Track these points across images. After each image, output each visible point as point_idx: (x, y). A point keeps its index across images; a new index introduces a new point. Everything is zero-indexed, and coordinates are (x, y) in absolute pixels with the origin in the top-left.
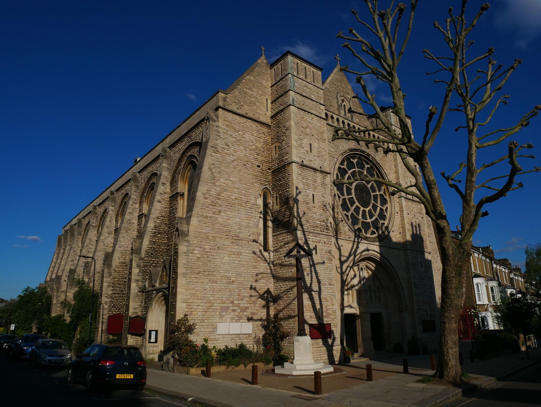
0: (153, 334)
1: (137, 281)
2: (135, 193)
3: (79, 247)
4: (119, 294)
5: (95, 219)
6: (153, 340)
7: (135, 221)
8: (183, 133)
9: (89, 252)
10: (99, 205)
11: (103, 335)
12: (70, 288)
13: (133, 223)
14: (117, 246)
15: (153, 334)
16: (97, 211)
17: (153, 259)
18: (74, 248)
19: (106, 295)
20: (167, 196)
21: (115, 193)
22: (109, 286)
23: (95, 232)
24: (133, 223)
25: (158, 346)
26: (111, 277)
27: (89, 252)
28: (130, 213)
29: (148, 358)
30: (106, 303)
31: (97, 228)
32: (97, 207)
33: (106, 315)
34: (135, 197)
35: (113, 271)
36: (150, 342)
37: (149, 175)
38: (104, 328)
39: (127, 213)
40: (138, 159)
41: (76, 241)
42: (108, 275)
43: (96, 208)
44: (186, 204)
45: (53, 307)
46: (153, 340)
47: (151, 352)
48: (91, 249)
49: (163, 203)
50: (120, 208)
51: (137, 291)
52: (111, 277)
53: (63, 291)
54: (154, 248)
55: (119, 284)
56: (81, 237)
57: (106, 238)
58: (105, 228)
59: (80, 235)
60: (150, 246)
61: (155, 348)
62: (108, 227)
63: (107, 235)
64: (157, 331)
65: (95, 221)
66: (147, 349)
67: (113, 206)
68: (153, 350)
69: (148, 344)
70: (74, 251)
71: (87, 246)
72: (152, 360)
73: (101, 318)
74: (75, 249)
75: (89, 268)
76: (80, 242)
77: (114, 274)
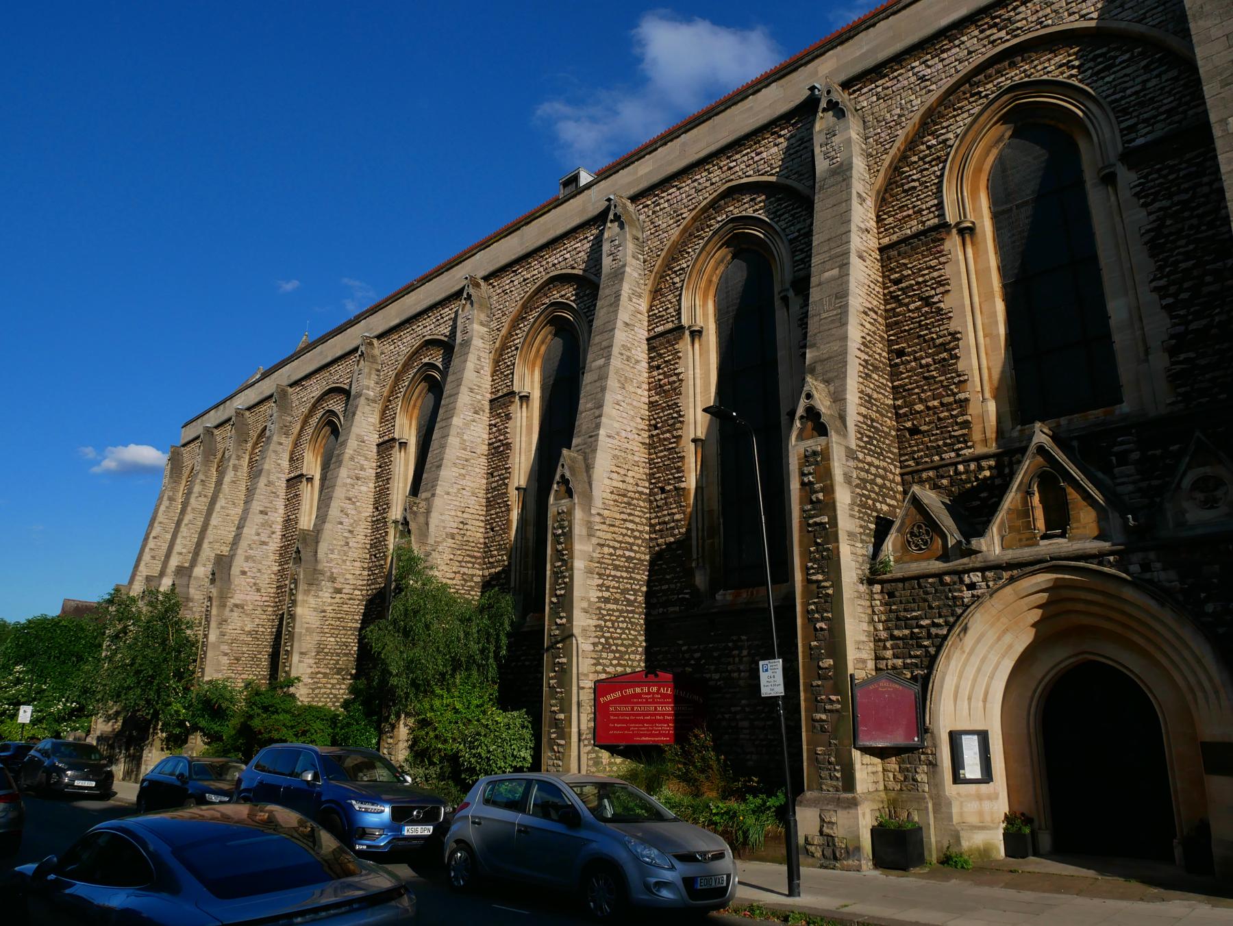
0: (970, 747)
1: (851, 535)
2: (634, 262)
3: (282, 471)
4: (616, 601)
5: (374, 377)
6: (972, 769)
7: (641, 352)
8: (944, 22)
9: (358, 479)
10: (379, 337)
11: (584, 750)
12: (307, 592)
13: (637, 362)
14: (602, 432)
15: (970, 747)
16: (376, 352)
17: (876, 462)
18: (269, 472)
19: (585, 605)
20: (873, 243)
21: (482, 283)
22: (590, 571)
23: (374, 418)
24: (637, 362)
25: (993, 797)
26: (595, 541)
27: (358, 479)
28: (627, 324)
29: (965, 844)
30: (584, 630)
31: (378, 407)
32: (375, 341)
33: (586, 675)
34: (636, 275)
35: (598, 519)
36: (957, 779)
37: (706, 197)
38: (584, 727)
39: (619, 324)
40: (585, 178)
41: (275, 452)
42: (584, 532)
43: (371, 344)
44: (993, 261)
45: (209, 654)
46: (972, 769)
47: (973, 820)
48: (362, 469)
49: (868, 262)
50: (514, 325)
51: (855, 579)
52: (595, 541)
53: (236, 606)
54: (872, 420)
55: (616, 568)
56: (288, 442)
57: (467, 425)
58: (464, 390)
59: (287, 434)
60: (863, 411)
61: (987, 805)
62: (471, 390)
63: (469, 415)
64: (983, 737)
65: (372, 384)
66: (955, 810)
67: (482, 324)
68: (981, 813)
69: (950, 789)
70: (269, 484)
71: (352, 459)
72: (985, 852)
73: (575, 689)
74: (273, 478)
75: (421, 519)
76: (286, 456)
77: (603, 533)
